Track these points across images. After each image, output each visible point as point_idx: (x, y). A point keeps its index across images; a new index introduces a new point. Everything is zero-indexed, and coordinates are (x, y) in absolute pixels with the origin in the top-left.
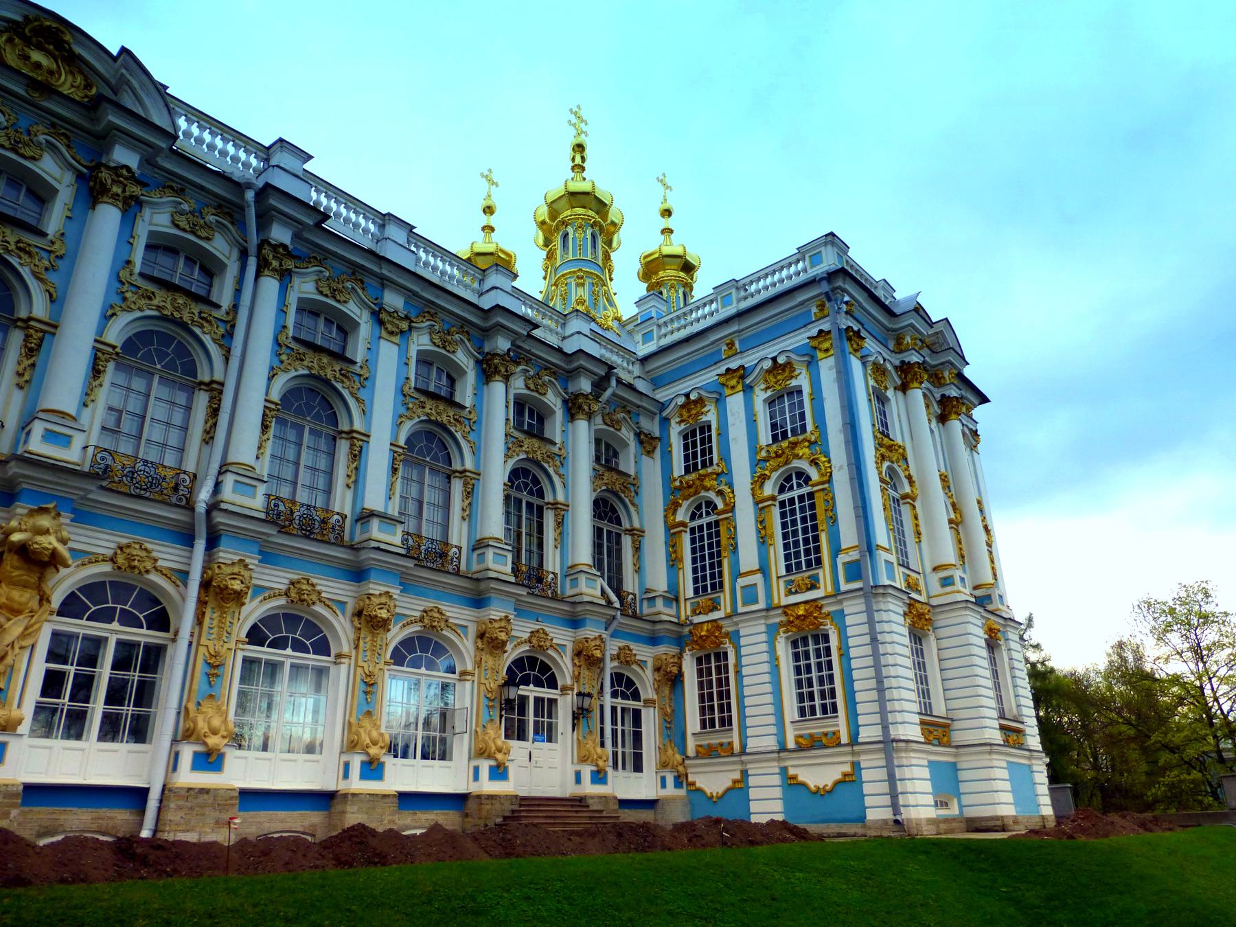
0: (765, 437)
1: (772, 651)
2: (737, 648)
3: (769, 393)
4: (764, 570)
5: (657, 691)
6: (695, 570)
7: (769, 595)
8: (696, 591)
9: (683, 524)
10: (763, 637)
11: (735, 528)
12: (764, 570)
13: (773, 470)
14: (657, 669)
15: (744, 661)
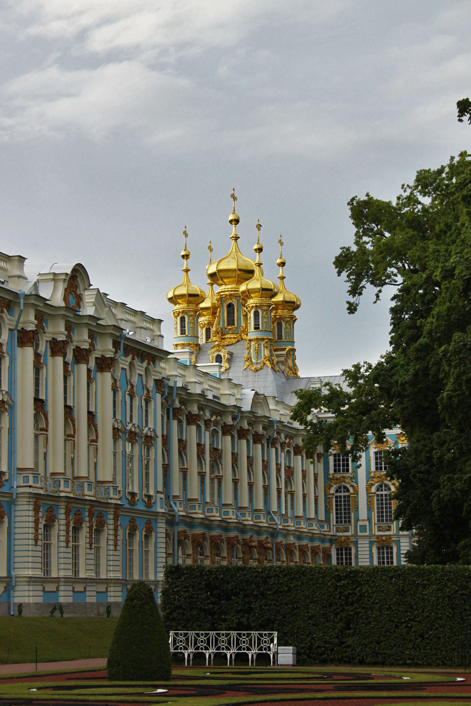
0: (373, 468)
1: (371, 550)
2: (357, 548)
3: (376, 450)
4: (369, 520)
5: (323, 561)
6: (337, 514)
7: (371, 529)
8: (337, 522)
9: (333, 494)
10: (368, 545)
11: (358, 501)
12: (369, 520)
13: (375, 482)
14: (324, 553)
15: (359, 553)
